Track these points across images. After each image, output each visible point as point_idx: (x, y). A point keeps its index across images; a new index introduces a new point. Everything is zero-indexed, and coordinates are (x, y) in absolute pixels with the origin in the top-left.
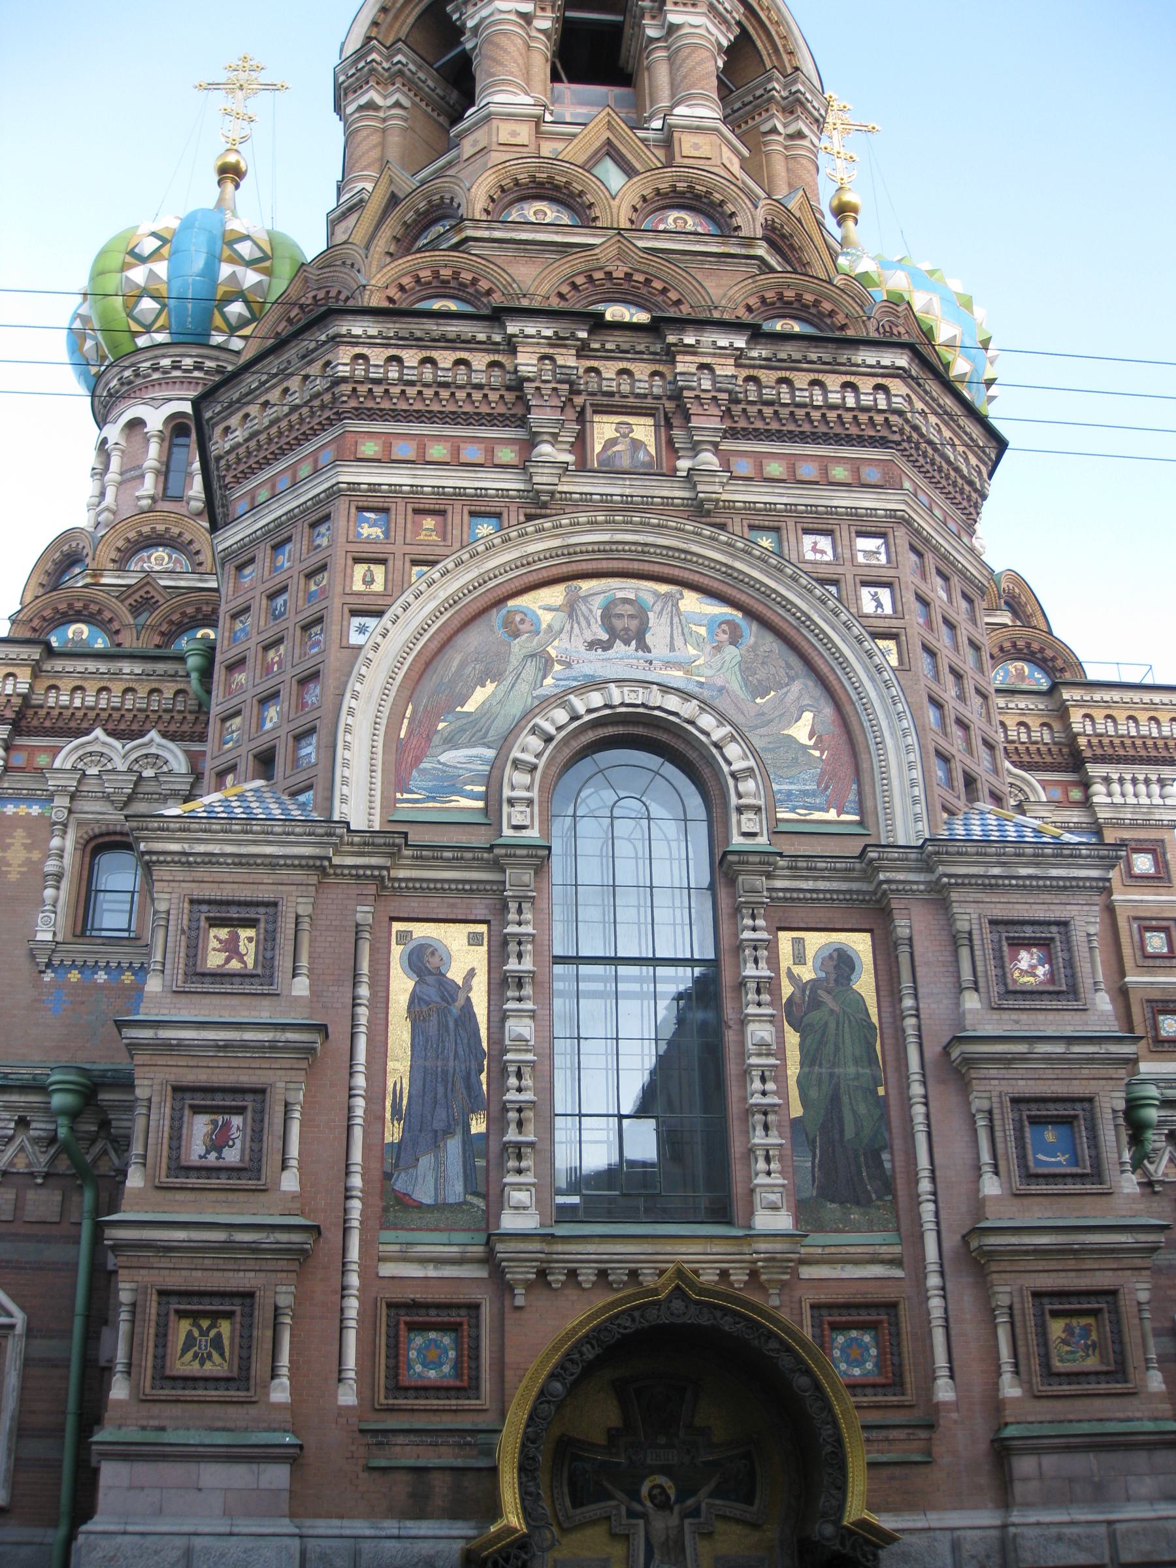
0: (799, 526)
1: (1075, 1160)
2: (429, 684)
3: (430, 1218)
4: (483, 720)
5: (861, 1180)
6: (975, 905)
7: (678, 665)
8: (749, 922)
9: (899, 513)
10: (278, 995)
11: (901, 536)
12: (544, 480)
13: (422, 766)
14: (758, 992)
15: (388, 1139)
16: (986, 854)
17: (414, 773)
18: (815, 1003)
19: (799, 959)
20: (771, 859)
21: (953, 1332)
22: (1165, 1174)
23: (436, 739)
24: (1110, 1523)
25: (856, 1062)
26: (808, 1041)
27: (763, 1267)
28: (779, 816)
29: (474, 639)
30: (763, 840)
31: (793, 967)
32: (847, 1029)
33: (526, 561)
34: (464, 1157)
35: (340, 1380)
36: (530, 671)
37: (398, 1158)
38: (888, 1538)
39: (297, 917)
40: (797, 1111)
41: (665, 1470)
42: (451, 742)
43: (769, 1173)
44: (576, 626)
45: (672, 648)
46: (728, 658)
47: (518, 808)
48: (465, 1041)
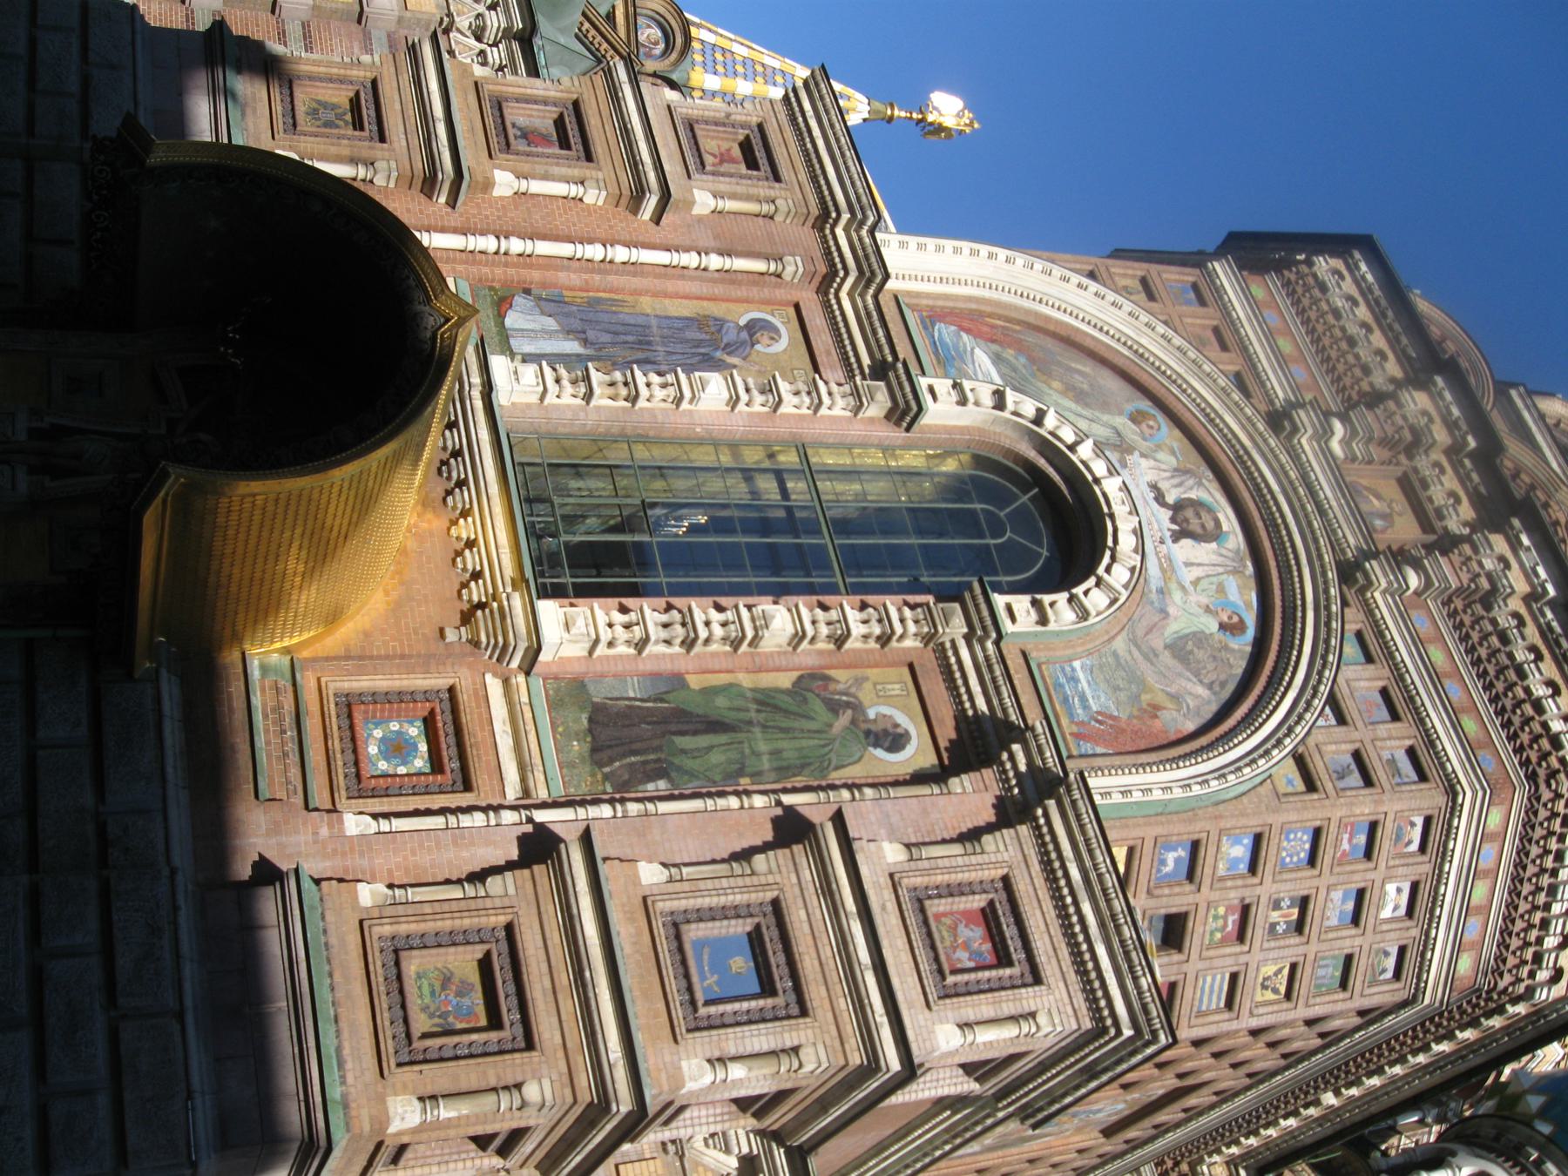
5: (624, 756)
6: (1020, 857)
9: (1458, 787)
10: (689, 177)
17: (953, 328)
18: (835, 707)
20: (991, 628)
23: (995, 347)
25: (775, 753)
27: (492, 612)
30: (1008, 626)
33: (1212, 418)
34: (563, 355)
37: (546, 300)
42: (997, 360)
44: (1168, 474)
45: (1188, 564)
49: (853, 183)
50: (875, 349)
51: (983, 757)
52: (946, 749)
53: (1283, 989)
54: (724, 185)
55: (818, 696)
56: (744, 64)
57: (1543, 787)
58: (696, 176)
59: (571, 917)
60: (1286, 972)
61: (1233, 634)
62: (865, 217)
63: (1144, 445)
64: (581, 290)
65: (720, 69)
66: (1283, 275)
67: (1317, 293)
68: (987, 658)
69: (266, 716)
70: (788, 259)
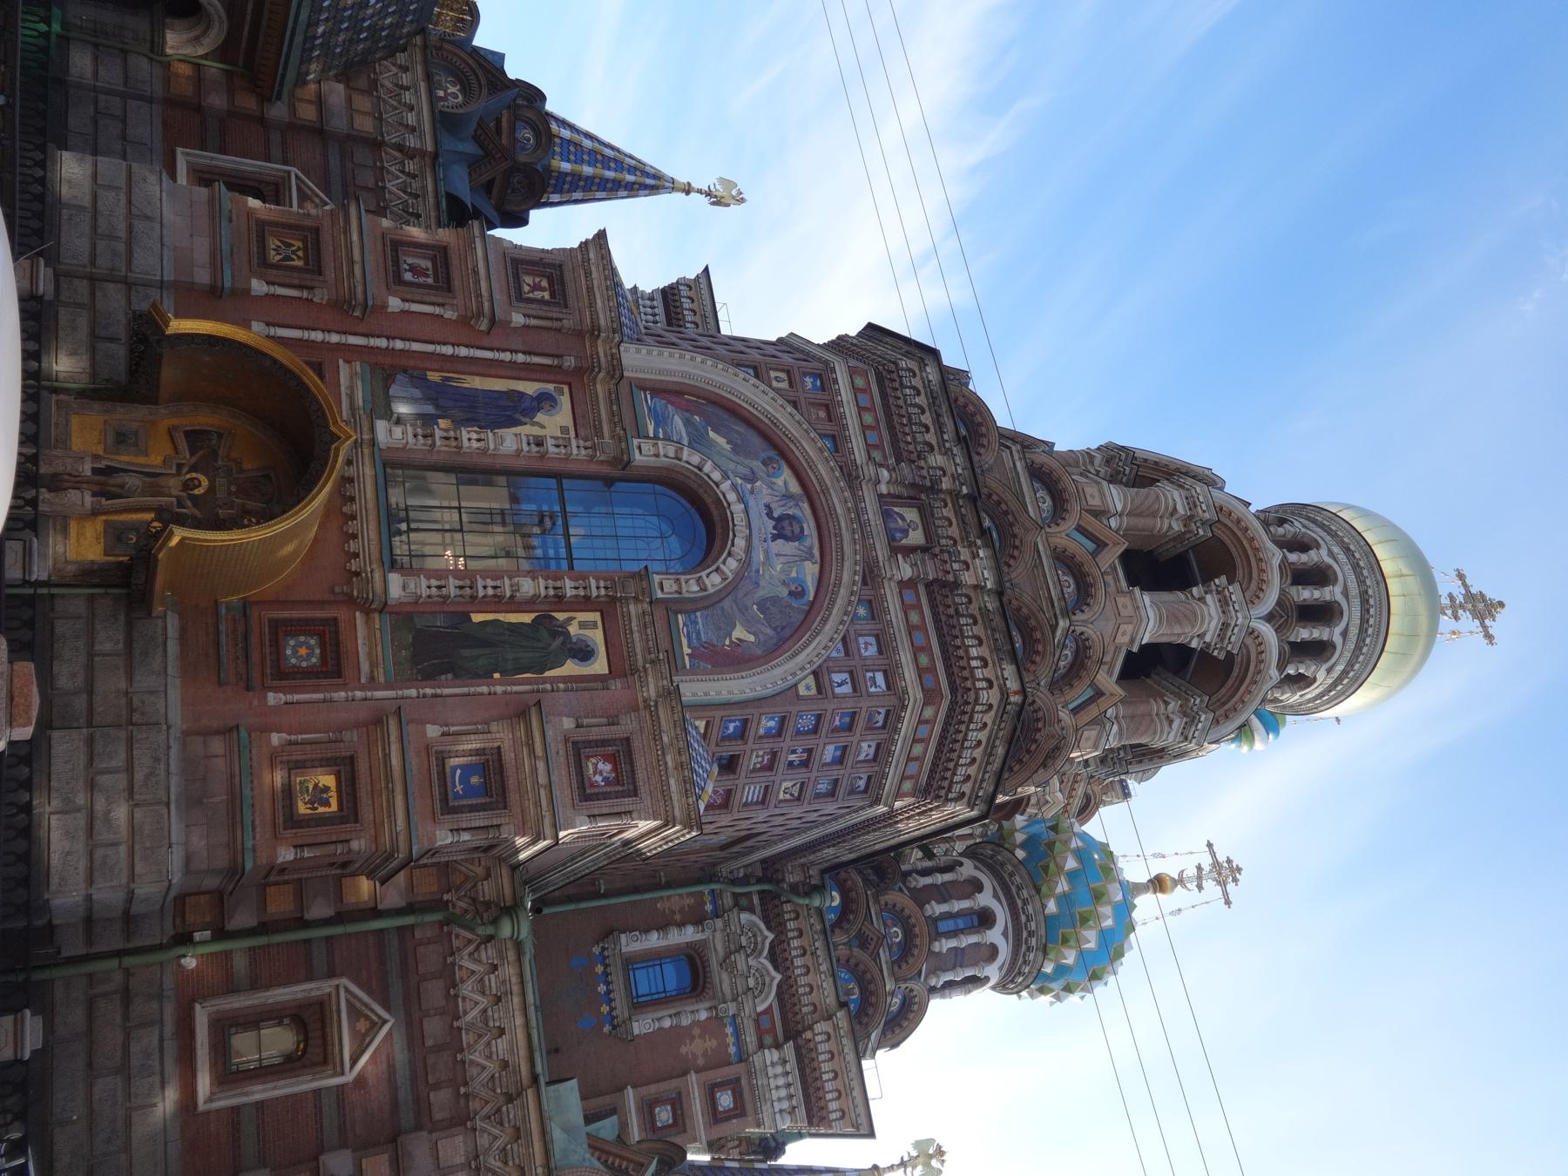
1: (457, 796)
2: (721, 412)
7: (767, 557)
8: (602, 584)
11: (893, 701)
12: (866, 471)
13: (670, 406)
14: (555, 588)
15: (428, 373)
17: (664, 402)
19: (583, 625)
22: (461, 967)
23: (687, 415)
24: (168, 805)
28: (679, 616)
29: (756, 440)
32: (537, 654)
36: (742, 470)
39: (561, 320)
40: (477, 618)
41: (212, 489)
53: (796, 794)
54: (533, 309)
56: (589, 154)
60: (798, 785)
61: (796, 598)
65: (572, 157)
69: (227, 636)
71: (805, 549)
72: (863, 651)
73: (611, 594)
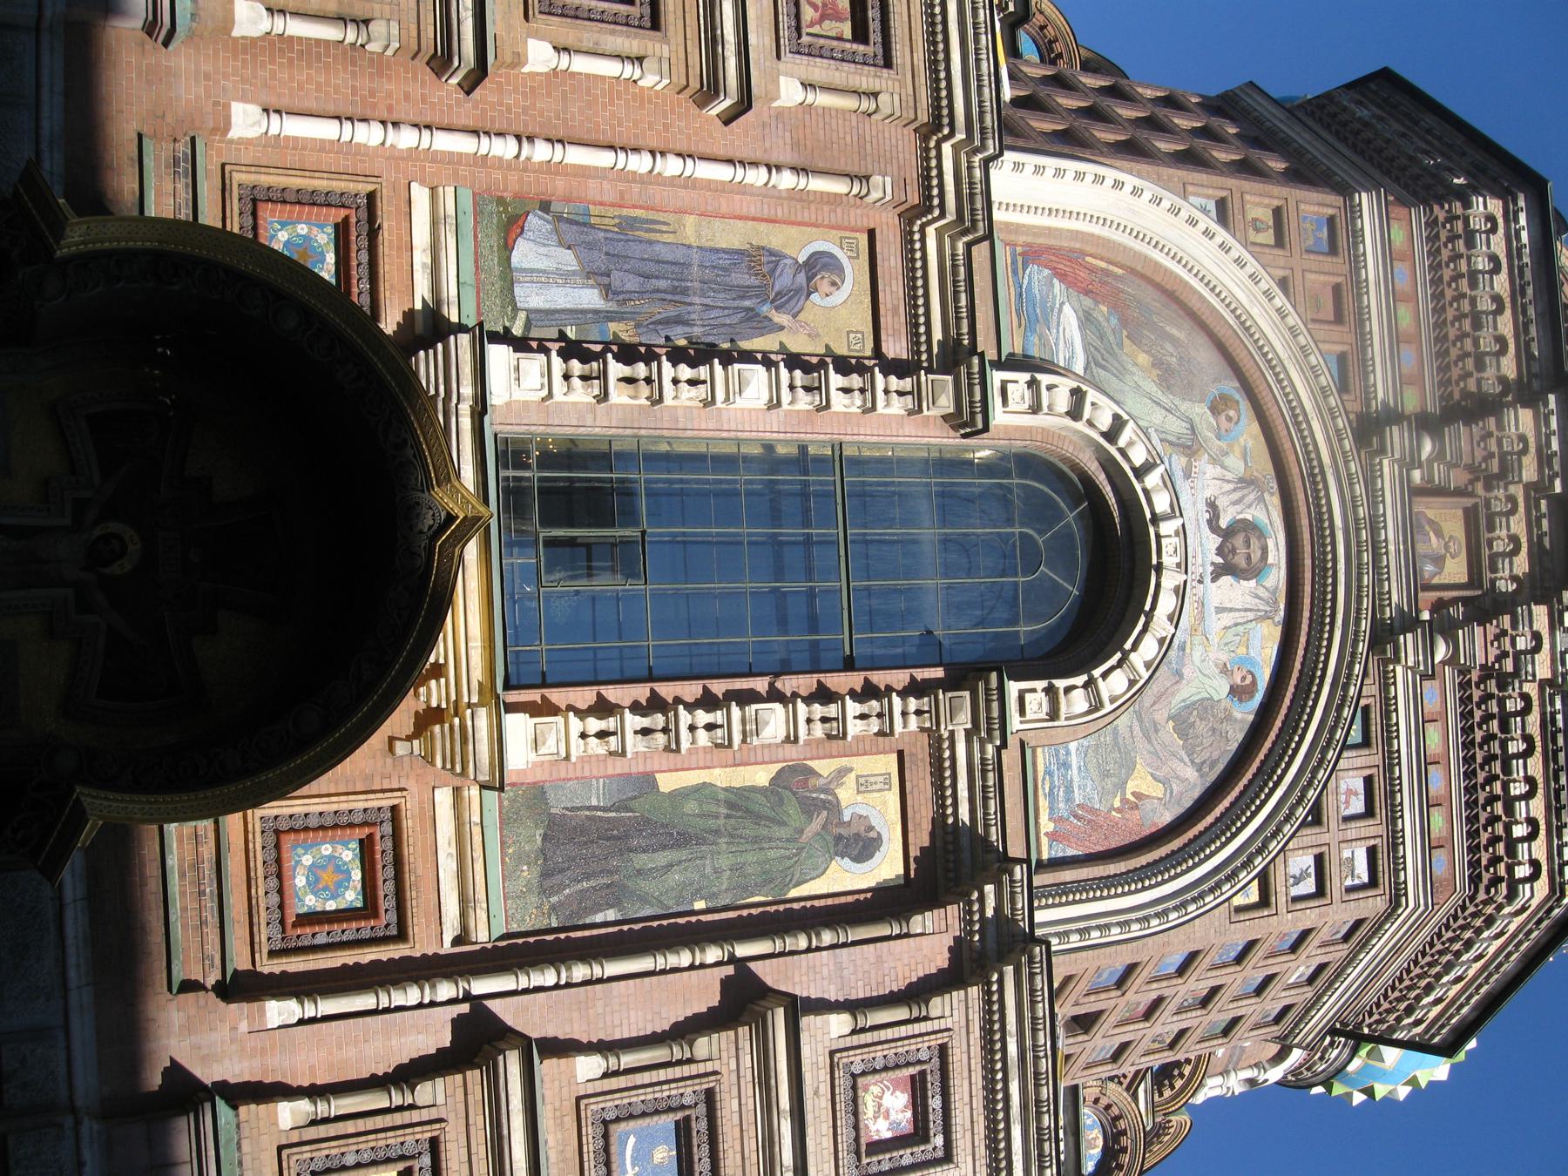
0: (1374, 771)
3: (493, 262)
4: (1116, 365)
6: (963, 1023)
10: (779, 57)
11: (1374, 904)
12: (1396, 440)
13: (1056, 281)
16: (1034, 1031)
17: (1047, 272)
18: (810, 808)
20: (997, 733)
21: (369, 1019)
23: (1088, 302)
26: (760, 798)
28: (1039, 750)
29: (1204, 356)
31: (853, 775)
33: (1299, 420)
35: (266, 110)
36: (1176, 426)
38: (51, 870)
40: (668, 783)
42: (1086, 320)
43: (583, 736)
44: (1231, 486)
45: (1220, 610)
46: (1215, 683)
47: (1028, 394)
48: (728, 322)
49: (980, 87)
50: (952, 322)
51: (951, 875)
52: (916, 859)
54: (820, 70)
55: (794, 794)
57: (1482, 888)
58: (787, 57)
59: (500, 1136)
62: (983, 147)
63: (1216, 444)
64: (613, 205)
66: (1432, 211)
67: (1460, 245)
68: (983, 760)
70: (877, 179)
71: (1265, 595)
72: (1343, 807)
73: (928, 725)
